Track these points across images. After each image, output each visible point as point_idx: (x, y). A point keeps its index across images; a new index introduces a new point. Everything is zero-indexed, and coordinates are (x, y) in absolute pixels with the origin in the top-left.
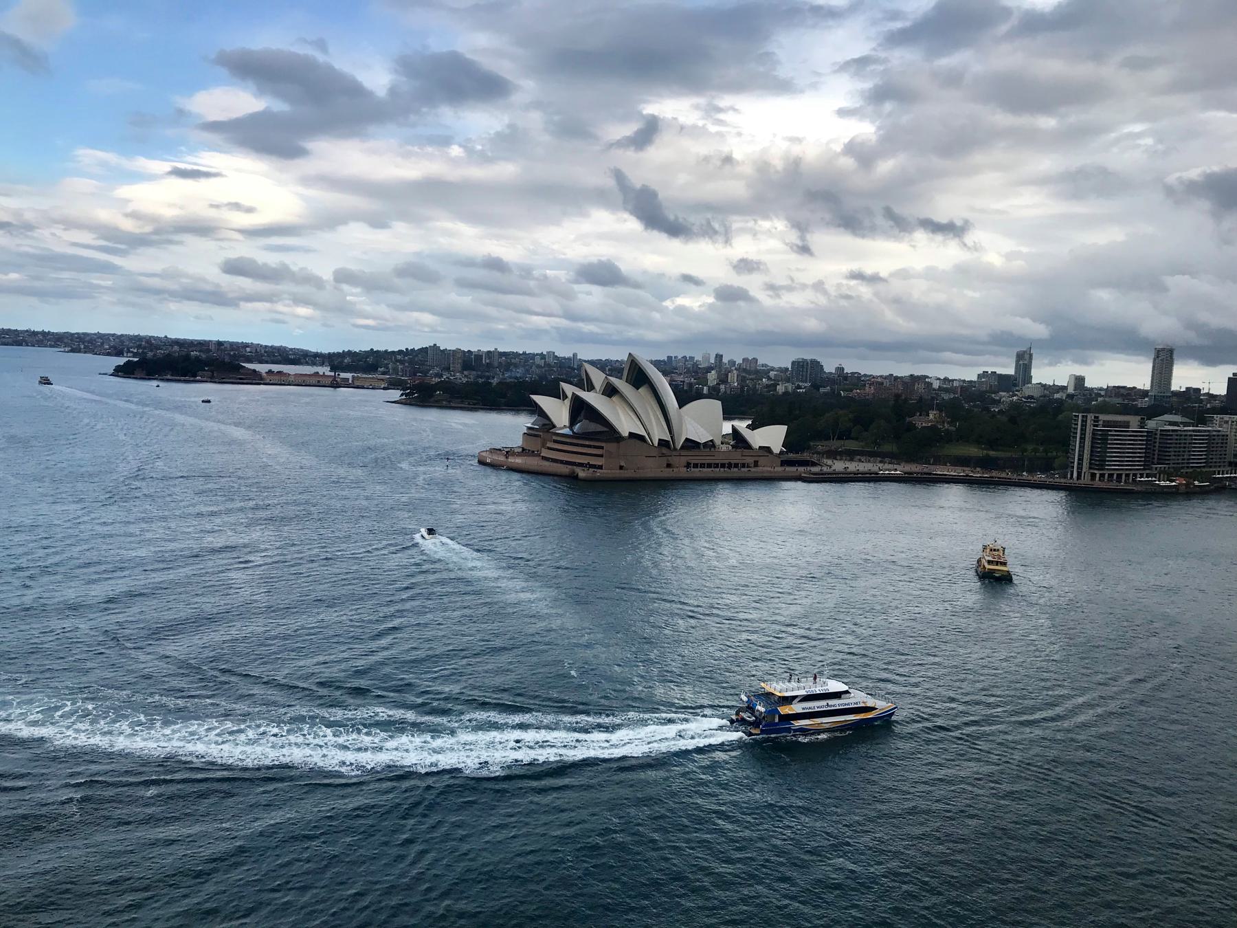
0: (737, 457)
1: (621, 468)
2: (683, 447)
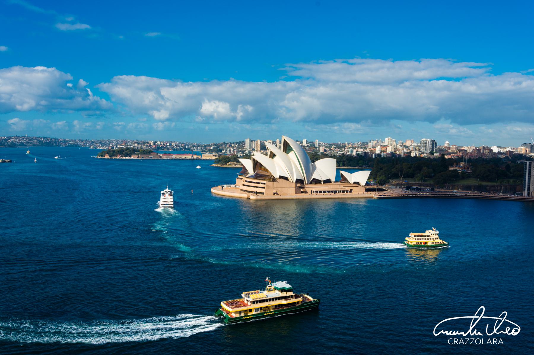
1: (274, 194)
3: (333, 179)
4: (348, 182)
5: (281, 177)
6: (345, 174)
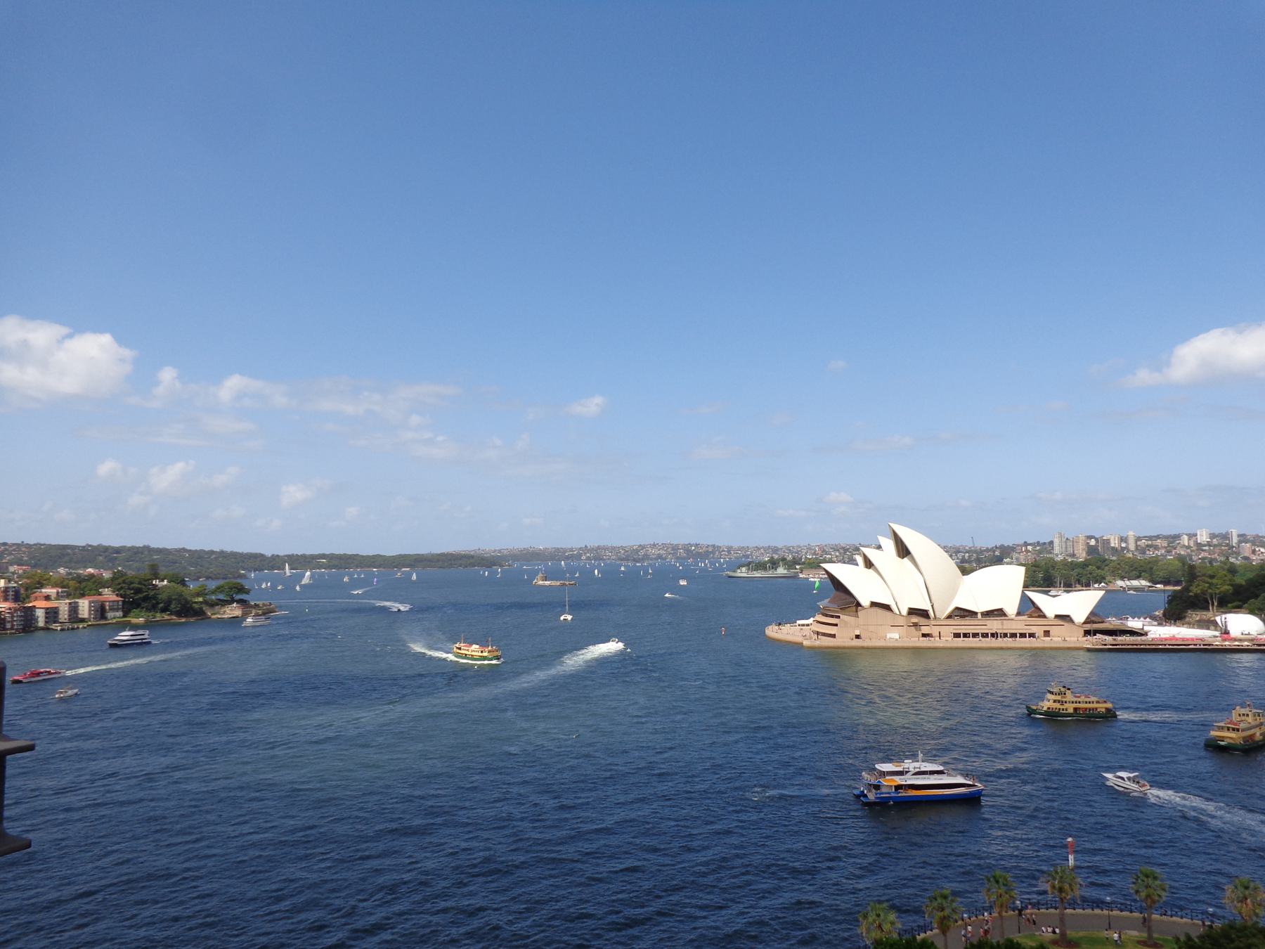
0: (1020, 625)
1: (858, 637)
2: (949, 617)
3: (1011, 610)
4: (1044, 616)
5: (874, 604)
6: (1038, 598)
